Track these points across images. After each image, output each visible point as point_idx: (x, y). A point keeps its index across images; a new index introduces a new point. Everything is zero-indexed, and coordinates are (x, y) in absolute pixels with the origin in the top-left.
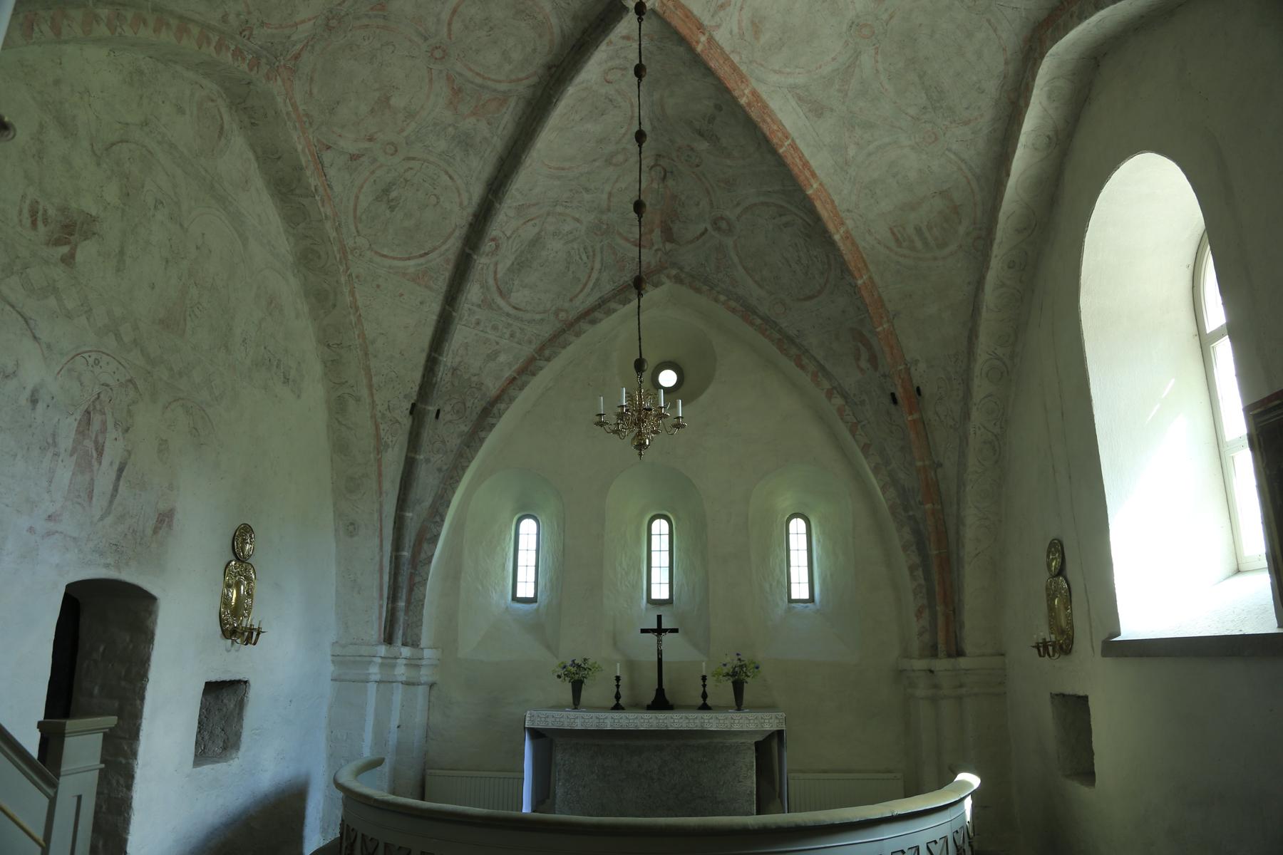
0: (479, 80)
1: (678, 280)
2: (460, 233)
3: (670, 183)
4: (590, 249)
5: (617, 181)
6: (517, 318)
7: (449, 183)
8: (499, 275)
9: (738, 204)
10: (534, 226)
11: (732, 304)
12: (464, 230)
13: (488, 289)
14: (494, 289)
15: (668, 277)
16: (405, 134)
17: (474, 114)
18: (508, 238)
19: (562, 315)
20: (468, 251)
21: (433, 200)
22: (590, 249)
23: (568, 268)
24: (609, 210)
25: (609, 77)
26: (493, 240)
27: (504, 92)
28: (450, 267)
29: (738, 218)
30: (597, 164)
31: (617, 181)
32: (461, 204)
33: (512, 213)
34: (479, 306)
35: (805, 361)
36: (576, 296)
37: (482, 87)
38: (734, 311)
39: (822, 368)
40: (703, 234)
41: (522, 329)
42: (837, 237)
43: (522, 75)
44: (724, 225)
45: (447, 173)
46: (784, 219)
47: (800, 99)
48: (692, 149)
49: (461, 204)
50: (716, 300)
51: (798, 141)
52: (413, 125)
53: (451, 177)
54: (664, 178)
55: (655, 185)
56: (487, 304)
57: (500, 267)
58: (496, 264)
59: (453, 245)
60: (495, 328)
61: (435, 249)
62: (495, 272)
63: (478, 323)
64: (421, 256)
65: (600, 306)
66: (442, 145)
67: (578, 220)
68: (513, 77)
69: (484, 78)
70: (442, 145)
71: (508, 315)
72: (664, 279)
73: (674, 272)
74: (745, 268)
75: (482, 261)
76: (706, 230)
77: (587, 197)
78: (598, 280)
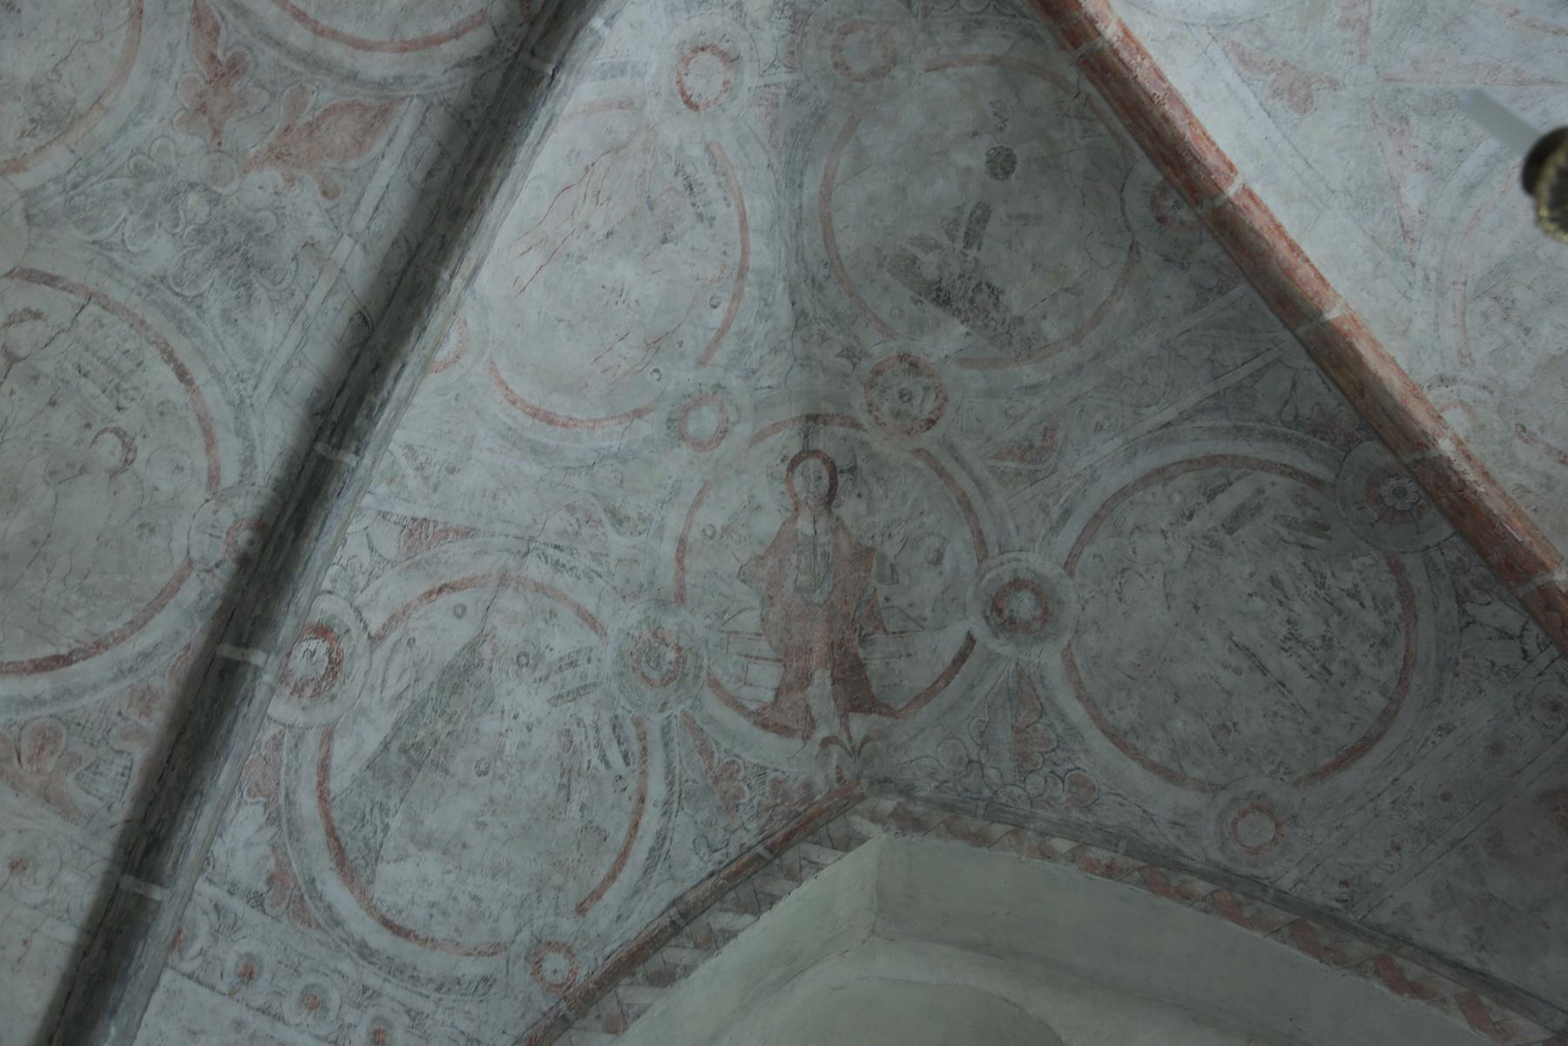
0: (299, 37)
1: (908, 822)
2: (201, 592)
3: (849, 507)
4: (631, 731)
5: (697, 504)
6: (396, 970)
7: (176, 393)
8: (336, 785)
9: (1067, 513)
10: (460, 612)
11: (1102, 855)
12: (217, 583)
13: (295, 833)
14: (316, 836)
15: (874, 818)
16: (25, 180)
17: (277, 155)
18: (375, 640)
19: (555, 964)
20: (226, 650)
21: (109, 450)
22: (631, 731)
23: (565, 789)
24: (681, 598)
25: (694, 84)
26: (323, 631)
27: (382, 85)
28: (155, 722)
29: (1069, 566)
30: (645, 428)
31: (697, 504)
32: (214, 478)
33: (390, 545)
34: (257, 901)
35: (1414, 972)
36: (597, 895)
37: (311, 61)
38: (1110, 871)
39: (1480, 979)
40: (961, 658)
41: (415, 1016)
42: (1446, 446)
43: (441, 26)
44: (1024, 605)
45: (169, 356)
46: (1226, 503)
47: (1244, 60)
48: (914, 366)
49: (214, 478)
50: (1048, 855)
51: (1257, 189)
52: (58, 159)
53: (182, 374)
54: (830, 499)
55: (804, 525)
56: (285, 893)
57: (342, 748)
58: (328, 735)
59: (173, 635)
60: (313, 1002)
61: (100, 646)
62: (324, 768)
63: (248, 974)
64: (40, 666)
65: (675, 929)
66: (160, 252)
67: (591, 621)
68: (412, 32)
69: (319, 32)
70: (160, 252)
71: (365, 952)
72: (861, 824)
73: (888, 804)
74: (1112, 734)
75: (275, 711)
76: (971, 640)
77: (620, 544)
78: (661, 837)
